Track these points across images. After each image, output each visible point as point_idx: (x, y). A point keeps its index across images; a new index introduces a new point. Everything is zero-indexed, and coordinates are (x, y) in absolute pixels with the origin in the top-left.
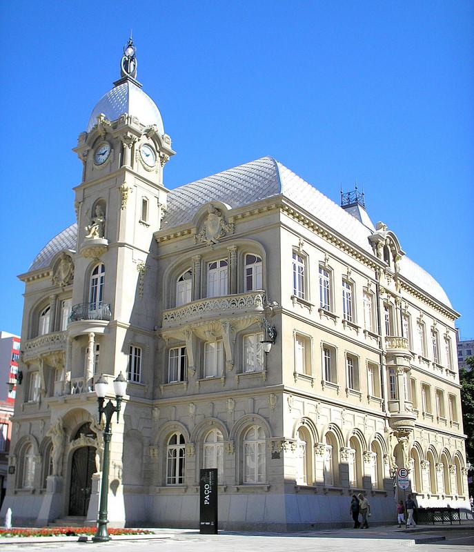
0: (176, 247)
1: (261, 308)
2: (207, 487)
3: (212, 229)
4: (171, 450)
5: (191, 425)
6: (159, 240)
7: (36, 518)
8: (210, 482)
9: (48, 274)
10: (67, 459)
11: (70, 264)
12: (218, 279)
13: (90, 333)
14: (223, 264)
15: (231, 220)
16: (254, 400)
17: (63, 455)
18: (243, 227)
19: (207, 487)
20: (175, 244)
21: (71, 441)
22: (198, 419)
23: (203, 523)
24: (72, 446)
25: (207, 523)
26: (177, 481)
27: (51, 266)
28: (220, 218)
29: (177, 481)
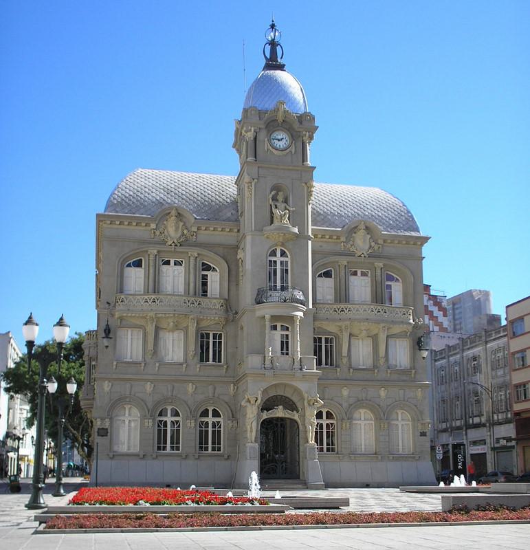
0: (321, 246)
1: (411, 321)
3: (361, 243)
5: (345, 405)
11: (181, 224)
12: (361, 287)
14: (364, 274)
15: (380, 242)
16: (405, 392)
17: (258, 424)
18: (390, 250)
20: (320, 244)
22: (352, 401)
24: (265, 415)
26: (325, 449)
27: (153, 219)
28: (369, 236)
29: (325, 449)
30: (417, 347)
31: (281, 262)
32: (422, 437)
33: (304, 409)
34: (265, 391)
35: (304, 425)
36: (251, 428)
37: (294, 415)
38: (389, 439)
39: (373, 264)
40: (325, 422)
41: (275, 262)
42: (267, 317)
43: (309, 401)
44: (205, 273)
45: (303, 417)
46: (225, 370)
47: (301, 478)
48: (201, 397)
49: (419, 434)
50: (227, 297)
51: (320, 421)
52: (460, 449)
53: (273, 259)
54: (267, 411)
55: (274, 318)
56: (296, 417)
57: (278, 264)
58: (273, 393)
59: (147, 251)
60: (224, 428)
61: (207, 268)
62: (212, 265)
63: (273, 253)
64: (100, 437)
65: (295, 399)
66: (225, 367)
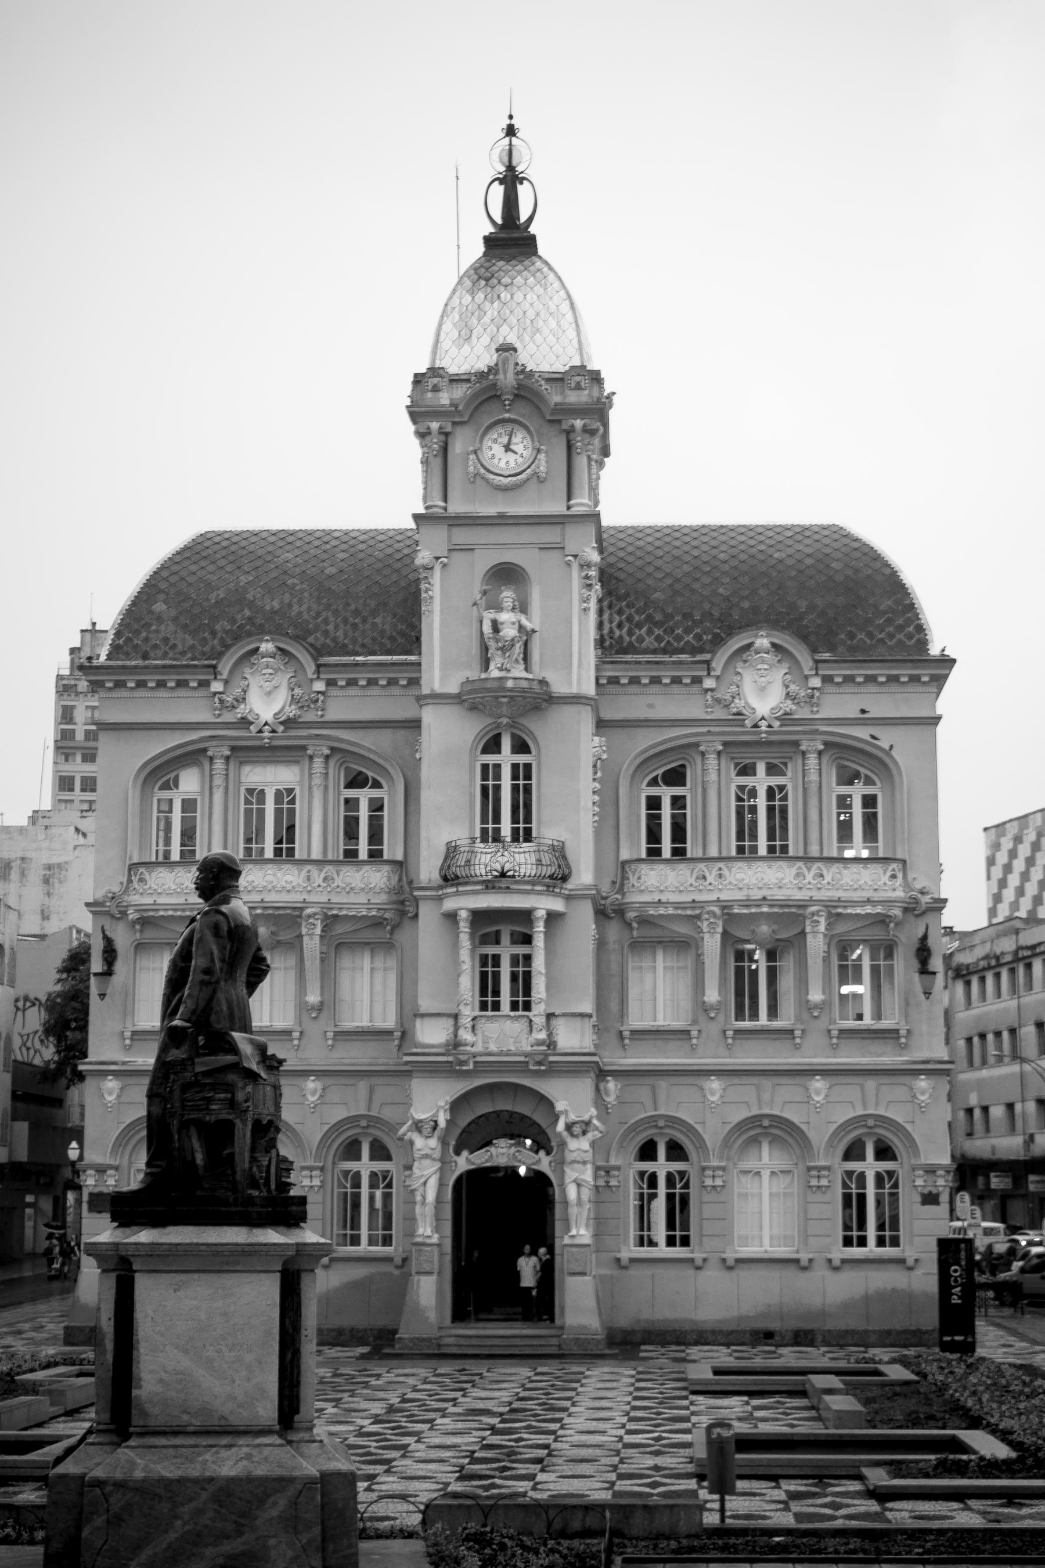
0: (651, 706)
2: (956, 1271)
4: (642, 1174)
6: (604, 681)
7: (395, 1332)
8: (963, 1263)
9: (204, 684)
10: (449, 1195)
13: (534, 909)
15: (816, 682)
17: (441, 1185)
19: (956, 1271)
21: (458, 1153)
23: (947, 1339)
24: (464, 1163)
25: (957, 1338)
30: (916, 964)
31: (515, 767)
32: (928, 1207)
33: (563, 1144)
34: (456, 1106)
35: (562, 1185)
36: (424, 1197)
37: (540, 1159)
38: (806, 1212)
39: (796, 744)
40: (662, 1167)
41: (498, 767)
42: (463, 914)
43: (569, 1127)
44: (352, 793)
45: (560, 1164)
46: (396, 1042)
47: (558, 1322)
48: (340, 1114)
49: (919, 1199)
50: (399, 857)
51: (648, 1166)
52: (959, 1251)
53: (491, 759)
54: (471, 1152)
55: (479, 917)
56: (544, 1163)
57: (506, 773)
58: (484, 1107)
59: (205, 750)
60: (397, 1189)
61: (357, 781)
62: (370, 774)
63: (493, 745)
64: (95, 1215)
65: (539, 1118)
66: (398, 1034)
